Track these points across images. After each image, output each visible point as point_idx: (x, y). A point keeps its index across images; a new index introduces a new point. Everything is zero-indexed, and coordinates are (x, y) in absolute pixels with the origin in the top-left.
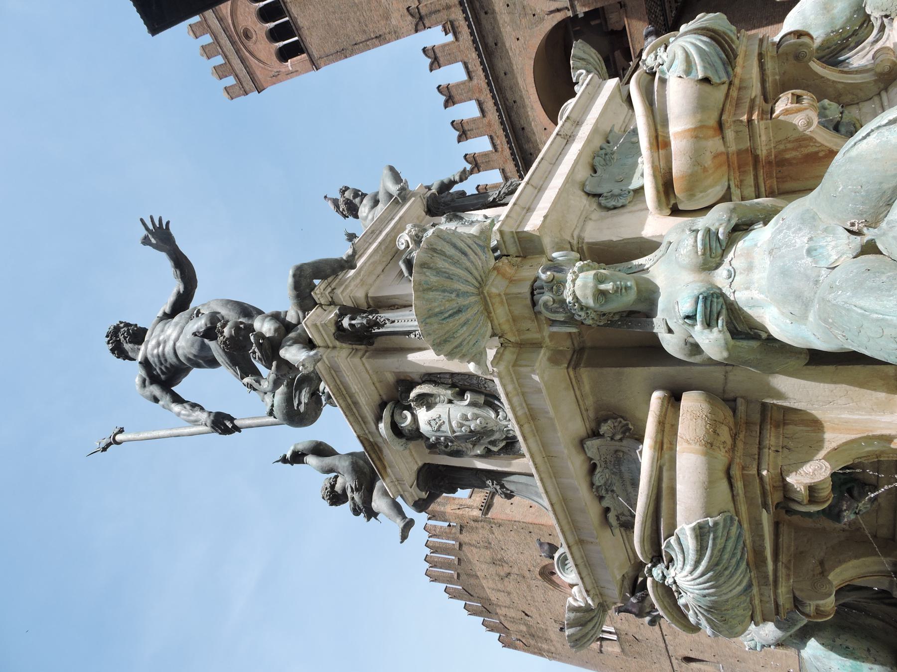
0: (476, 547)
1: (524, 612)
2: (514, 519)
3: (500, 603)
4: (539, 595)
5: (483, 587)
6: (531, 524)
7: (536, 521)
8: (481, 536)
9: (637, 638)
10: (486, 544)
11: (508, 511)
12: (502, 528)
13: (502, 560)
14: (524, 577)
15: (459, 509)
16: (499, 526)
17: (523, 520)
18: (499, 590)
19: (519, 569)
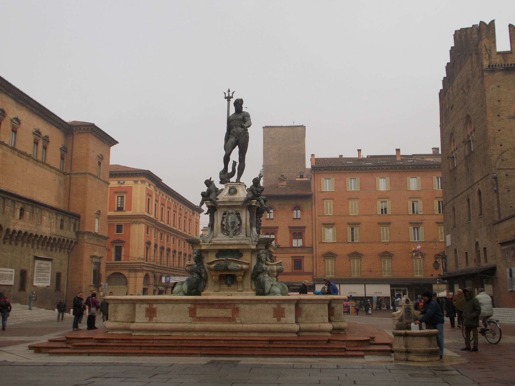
0: (472, 67)
1: (453, 106)
6: (486, 106)
9: (456, 180)
12: (481, 84)
13: (468, 87)
14: (465, 104)
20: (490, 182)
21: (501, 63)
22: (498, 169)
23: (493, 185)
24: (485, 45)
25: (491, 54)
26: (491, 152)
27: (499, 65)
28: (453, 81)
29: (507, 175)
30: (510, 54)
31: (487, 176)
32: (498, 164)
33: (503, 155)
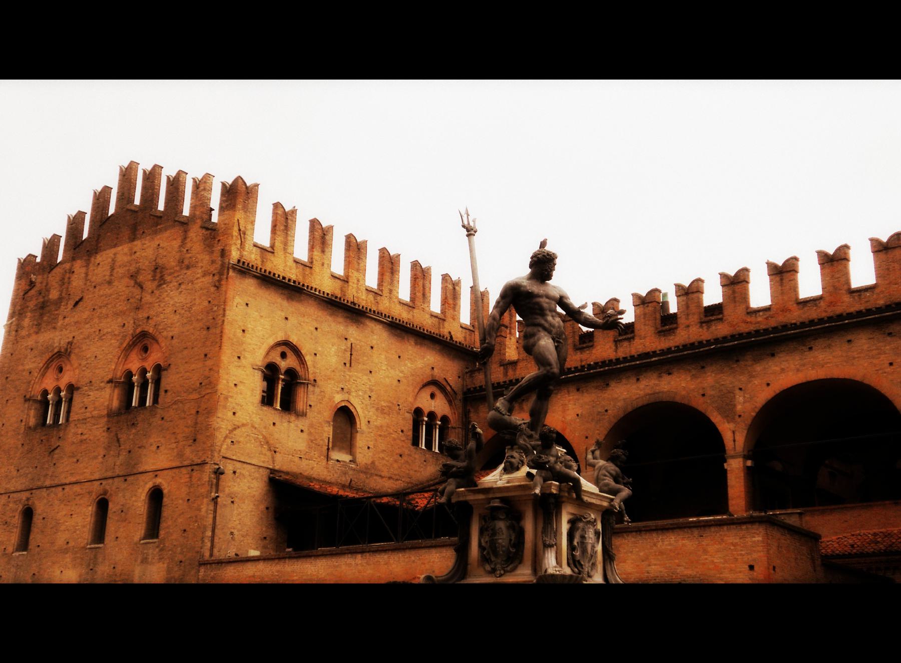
0: (181, 246)
2: (227, 308)
3: (91, 268)
4: (112, 326)
5: (115, 246)
6: (222, 332)
7: (225, 338)
8: (200, 257)
10: (186, 262)
11: (238, 300)
12: (213, 289)
14: (138, 308)
15: (240, 230)
16: (215, 286)
17: (226, 321)
18: (112, 269)
19: (150, 303)
20: (207, 479)
21: (257, 264)
22: (223, 457)
23: (212, 485)
24: (238, 220)
25: (245, 242)
26: (218, 423)
27: (253, 266)
28: (97, 253)
29: (234, 472)
30: (270, 254)
31: (197, 465)
32: (225, 446)
33: (235, 432)
